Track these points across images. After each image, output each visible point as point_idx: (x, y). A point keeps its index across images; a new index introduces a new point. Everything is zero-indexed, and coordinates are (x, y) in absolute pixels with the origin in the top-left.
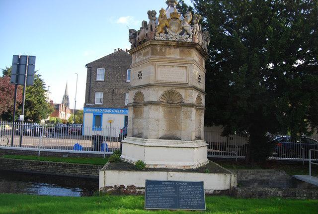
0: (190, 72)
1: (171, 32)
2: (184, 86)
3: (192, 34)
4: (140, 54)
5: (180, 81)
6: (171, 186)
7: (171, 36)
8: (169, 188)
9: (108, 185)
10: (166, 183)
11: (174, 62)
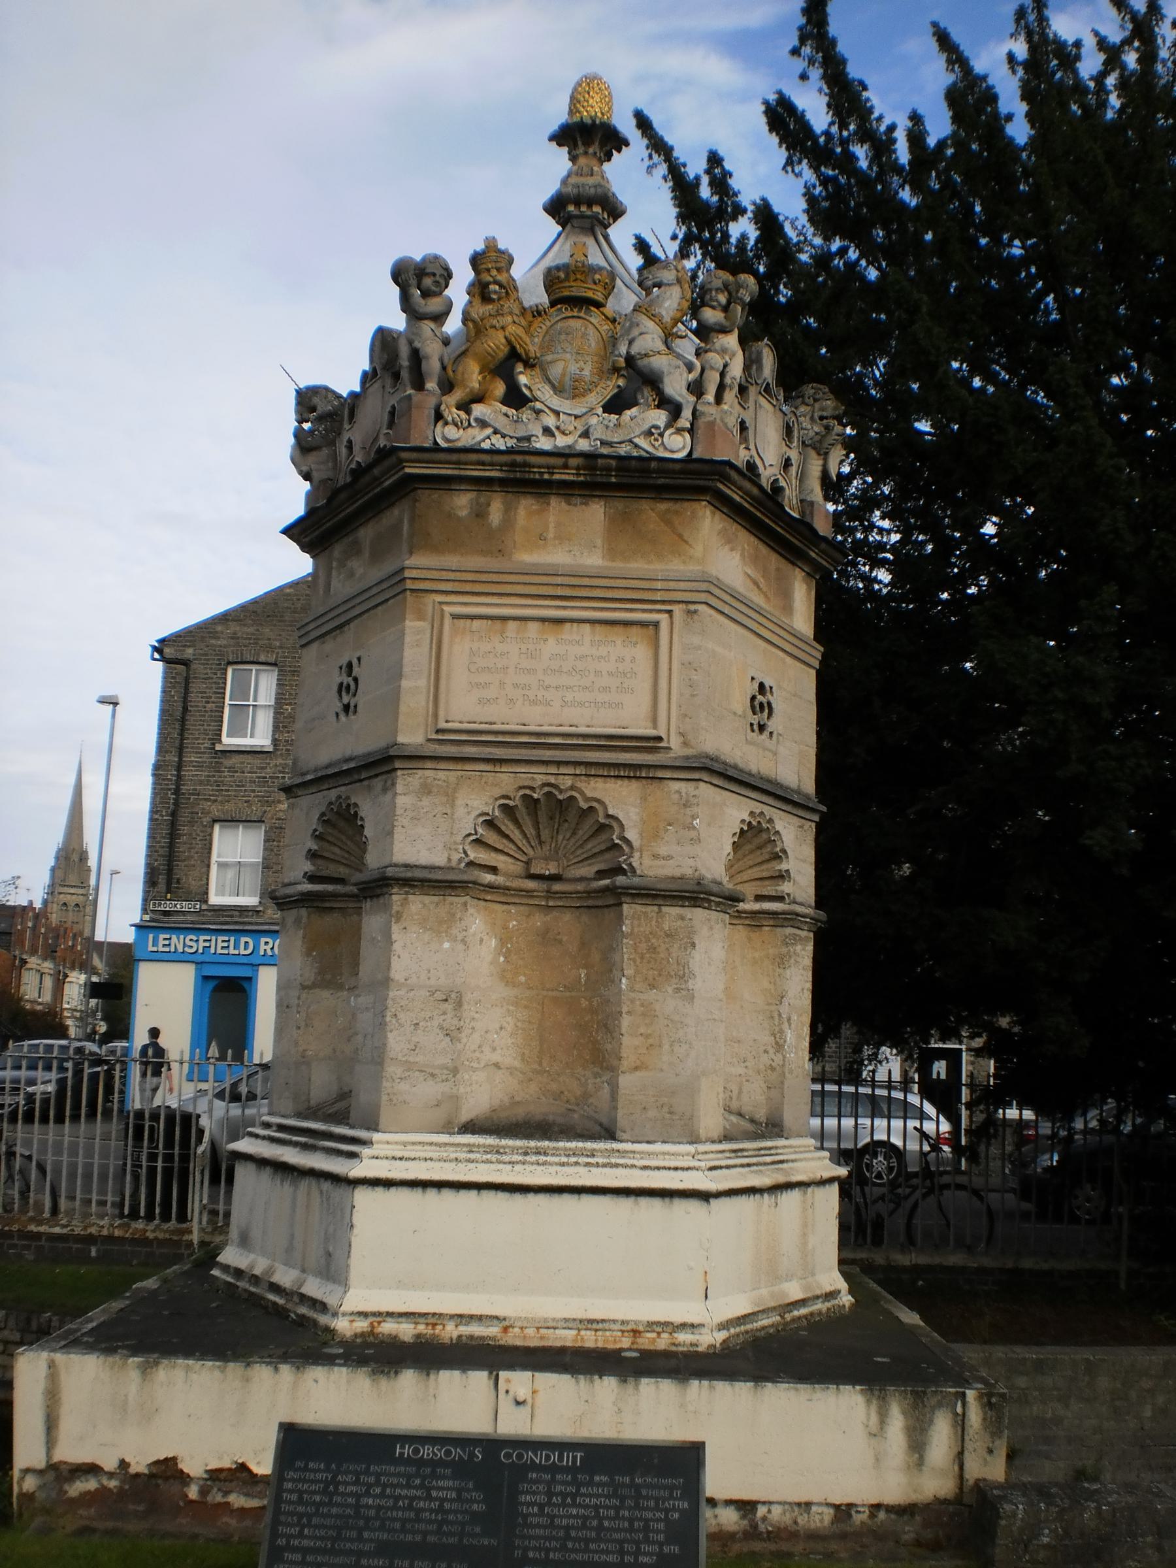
0: (700, 675)
1: (545, 393)
2: (636, 758)
3: (687, 400)
4: (355, 550)
5: (604, 722)
6: (461, 1469)
7: (550, 421)
8: (445, 1487)
9: (69, 1452)
10: (426, 1452)
11: (567, 600)
